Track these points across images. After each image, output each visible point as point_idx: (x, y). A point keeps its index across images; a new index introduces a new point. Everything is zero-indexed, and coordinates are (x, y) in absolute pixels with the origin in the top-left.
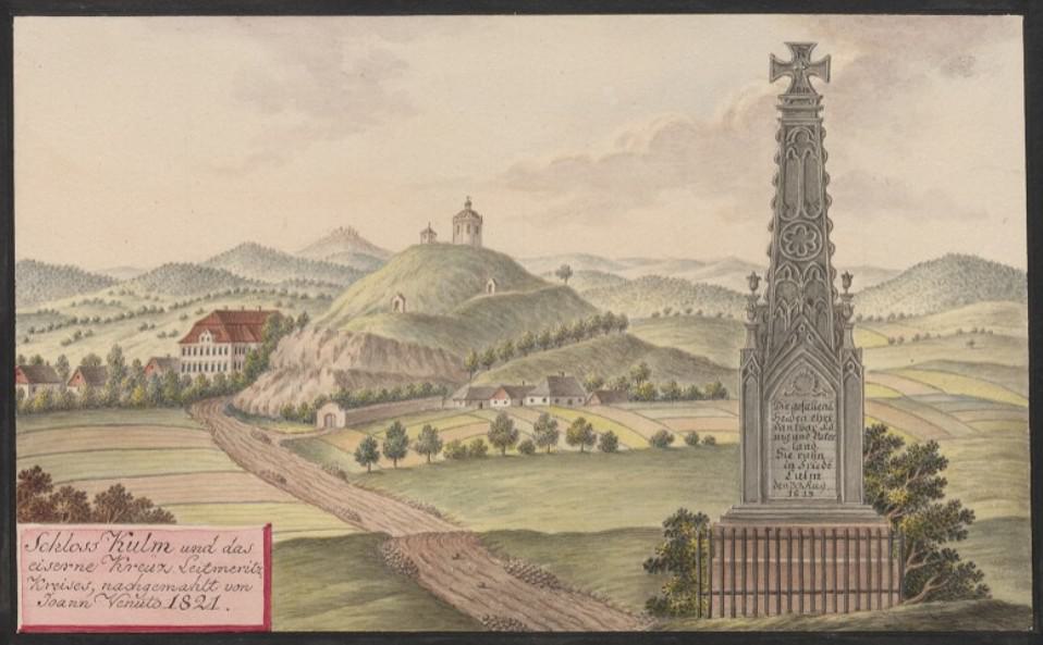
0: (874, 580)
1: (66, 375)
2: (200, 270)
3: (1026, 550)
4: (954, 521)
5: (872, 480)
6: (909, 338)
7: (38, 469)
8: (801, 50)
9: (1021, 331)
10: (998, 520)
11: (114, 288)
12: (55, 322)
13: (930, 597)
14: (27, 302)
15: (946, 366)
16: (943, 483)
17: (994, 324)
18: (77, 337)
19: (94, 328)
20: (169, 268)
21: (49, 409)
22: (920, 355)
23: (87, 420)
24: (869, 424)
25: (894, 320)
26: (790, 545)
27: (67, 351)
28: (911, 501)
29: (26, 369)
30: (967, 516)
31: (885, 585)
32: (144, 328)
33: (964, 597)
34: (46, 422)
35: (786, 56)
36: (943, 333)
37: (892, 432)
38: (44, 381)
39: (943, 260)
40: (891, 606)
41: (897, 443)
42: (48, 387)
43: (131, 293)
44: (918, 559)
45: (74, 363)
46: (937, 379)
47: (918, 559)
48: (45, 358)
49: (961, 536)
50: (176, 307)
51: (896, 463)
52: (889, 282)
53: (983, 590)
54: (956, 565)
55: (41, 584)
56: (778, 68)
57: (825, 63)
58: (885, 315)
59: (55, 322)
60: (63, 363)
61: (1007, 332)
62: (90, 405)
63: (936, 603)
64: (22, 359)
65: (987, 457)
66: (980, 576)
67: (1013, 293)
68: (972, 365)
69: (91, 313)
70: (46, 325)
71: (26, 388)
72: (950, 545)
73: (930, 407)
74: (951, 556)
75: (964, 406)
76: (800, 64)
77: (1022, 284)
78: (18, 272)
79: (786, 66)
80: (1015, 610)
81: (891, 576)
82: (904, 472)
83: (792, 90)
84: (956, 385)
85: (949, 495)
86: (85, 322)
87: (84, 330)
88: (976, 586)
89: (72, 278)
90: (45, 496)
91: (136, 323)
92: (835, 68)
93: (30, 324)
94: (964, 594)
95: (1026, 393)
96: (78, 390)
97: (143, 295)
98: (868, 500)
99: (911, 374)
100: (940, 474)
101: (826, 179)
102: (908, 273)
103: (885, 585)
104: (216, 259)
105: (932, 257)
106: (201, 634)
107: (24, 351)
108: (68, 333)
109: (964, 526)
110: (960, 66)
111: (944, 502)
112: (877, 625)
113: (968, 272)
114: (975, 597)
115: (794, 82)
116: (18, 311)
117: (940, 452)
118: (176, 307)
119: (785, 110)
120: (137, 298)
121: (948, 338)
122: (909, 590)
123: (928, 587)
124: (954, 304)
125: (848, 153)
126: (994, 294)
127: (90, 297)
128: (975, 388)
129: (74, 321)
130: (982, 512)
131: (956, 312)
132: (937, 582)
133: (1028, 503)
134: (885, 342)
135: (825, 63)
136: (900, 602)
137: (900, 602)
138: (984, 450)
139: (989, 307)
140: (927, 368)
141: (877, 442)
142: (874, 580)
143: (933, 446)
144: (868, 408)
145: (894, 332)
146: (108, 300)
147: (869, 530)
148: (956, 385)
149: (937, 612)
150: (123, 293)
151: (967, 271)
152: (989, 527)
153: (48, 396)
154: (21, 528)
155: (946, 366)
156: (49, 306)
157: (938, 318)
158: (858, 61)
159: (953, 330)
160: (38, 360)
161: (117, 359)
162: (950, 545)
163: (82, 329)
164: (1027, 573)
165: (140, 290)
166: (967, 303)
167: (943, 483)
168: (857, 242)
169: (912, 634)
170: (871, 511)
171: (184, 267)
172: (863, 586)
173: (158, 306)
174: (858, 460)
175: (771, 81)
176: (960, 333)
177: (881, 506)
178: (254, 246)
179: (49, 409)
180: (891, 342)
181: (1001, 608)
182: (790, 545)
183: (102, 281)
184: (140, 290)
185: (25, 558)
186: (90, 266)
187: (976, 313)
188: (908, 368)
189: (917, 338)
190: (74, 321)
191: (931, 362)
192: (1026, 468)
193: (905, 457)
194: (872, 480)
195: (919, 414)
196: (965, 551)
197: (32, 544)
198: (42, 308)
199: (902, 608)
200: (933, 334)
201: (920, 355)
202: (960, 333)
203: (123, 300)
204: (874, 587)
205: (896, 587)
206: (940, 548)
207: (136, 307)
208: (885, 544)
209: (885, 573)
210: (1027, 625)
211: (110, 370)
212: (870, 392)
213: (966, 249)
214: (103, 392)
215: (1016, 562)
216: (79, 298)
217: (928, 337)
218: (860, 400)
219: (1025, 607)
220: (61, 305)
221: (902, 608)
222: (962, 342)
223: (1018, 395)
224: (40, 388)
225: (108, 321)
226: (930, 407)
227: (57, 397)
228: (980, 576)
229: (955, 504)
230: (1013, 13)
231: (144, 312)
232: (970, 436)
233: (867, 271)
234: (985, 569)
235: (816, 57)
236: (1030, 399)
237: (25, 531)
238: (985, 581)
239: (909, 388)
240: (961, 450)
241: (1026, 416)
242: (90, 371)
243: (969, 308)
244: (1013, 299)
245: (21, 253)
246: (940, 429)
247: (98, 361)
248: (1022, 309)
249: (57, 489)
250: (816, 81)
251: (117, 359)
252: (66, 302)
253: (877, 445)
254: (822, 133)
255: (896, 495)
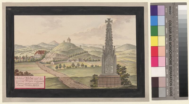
0: (118, 83)
1: (20, 58)
2: (37, 46)
3: (136, 79)
4: (127, 76)
5: (118, 71)
6: (122, 54)
7: (17, 69)
8: (109, 19)
9: (136, 53)
10: (133, 75)
11: (26, 48)
12: (19, 52)
13: (125, 85)
14: (16, 49)
15: (127, 57)
16: (126, 71)
17: (132, 52)
18: (22, 54)
19: (24, 53)
20: (33, 46)
21: (18, 62)
22: (123, 56)
23: (23, 63)
24: (117, 64)
25: (120, 52)
26: (102, 78)
27: (21, 55)
28: (122, 73)
29: (16, 57)
30: (129, 75)
31: (119, 83)
32: (30, 52)
33: (129, 85)
34: (18, 64)
35: (107, 20)
36: (126, 53)
37: (120, 65)
38: (18, 59)
39: (126, 44)
40: (120, 86)
41: (120, 66)
42: (18, 60)
43: (28, 48)
44: (123, 80)
45: (21, 57)
46: (125, 59)
47: (123, 80)
48: (18, 56)
49: (128, 77)
50: (34, 50)
51: (120, 69)
52: (119, 47)
53: (131, 84)
54: (128, 81)
55: (17, 83)
56: (106, 21)
57: (112, 21)
58: (119, 51)
59: (19, 52)
60: (20, 57)
61: (134, 53)
62: (23, 62)
63: (125, 85)
64: (15, 56)
65: (131, 68)
66: (131, 82)
67: (134, 48)
68: (129, 57)
69: (23, 51)
70: (18, 52)
71: (16, 60)
72: (127, 78)
73: (125, 62)
74: (127, 80)
75: (128, 62)
76: (109, 21)
77: (136, 47)
78: (15, 46)
79: (107, 21)
80: (135, 86)
81: (120, 82)
82: (121, 70)
83: (108, 24)
84: (128, 59)
85: (127, 73)
86: (23, 52)
87: (23, 53)
88: (130, 83)
89: (21, 46)
90: (18, 73)
91: (29, 52)
92: (113, 21)
93: (16, 52)
94: (129, 84)
95: (136, 60)
96: (22, 60)
97: (30, 48)
98: (117, 73)
99: (122, 58)
100: (126, 70)
101: (112, 35)
102: (122, 46)
103: (119, 83)
104: (39, 44)
105: (125, 44)
106: (67, 86)
107: (15, 55)
108: (21, 53)
109: (129, 76)
110: (128, 21)
111: (126, 73)
112: (118, 88)
113: (129, 46)
114: (130, 85)
115: (108, 23)
116: (15, 51)
117: (126, 67)
118: (34, 50)
119: (107, 27)
120: (29, 49)
121: (127, 54)
122: (122, 84)
123: (124, 84)
124: (127, 50)
125: (115, 32)
126: (132, 48)
127: (23, 49)
128: (130, 60)
129: (21, 52)
130: (131, 74)
131: (128, 51)
132: (125, 83)
133: (136, 73)
134: (119, 54)
135: (112, 21)
136: (121, 85)
137: (121, 85)
138: (131, 67)
139: (132, 50)
140: (124, 57)
141: (118, 66)
142: (118, 83)
143: (125, 67)
144: (117, 62)
145: (120, 53)
146: (25, 49)
147: (117, 77)
148: (128, 59)
149: (125, 86)
150: (27, 48)
151: (129, 46)
152: (132, 76)
153: (18, 61)
154: (15, 76)
155: (127, 57)
156: (18, 50)
157: (125, 51)
158: (116, 21)
159: (127, 53)
160: (17, 56)
161: (27, 56)
162: (127, 78)
163: (22, 52)
164: (136, 82)
165: (29, 48)
166: (129, 50)
167: (126, 71)
168: (116, 42)
169: (122, 89)
170: (117, 74)
171: (35, 45)
172: (117, 83)
173: (32, 50)
174: (116, 68)
175: (106, 23)
176: (128, 53)
177: (119, 74)
178: (43, 43)
179: (18, 62)
180: (120, 54)
181: (133, 86)
182: (102, 78)
183: (25, 47)
184: (29, 48)
185: (16, 80)
186: (23, 45)
187: (130, 51)
188: (122, 57)
189: (123, 54)
190: (21, 52)
191: (124, 57)
192: (136, 69)
193: (121, 68)
194: (118, 71)
195: (123, 63)
196: (129, 79)
197: (16, 78)
198: (18, 50)
199: (121, 86)
200: (125, 53)
201: (123, 56)
202: (128, 53)
203: (28, 49)
204: (118, 83)
205: (120, 83)
206: (126, 79)
207: (29, 50)
208: (119, 78)
209: (119, 82)
210: (136, 88)
211: (26, 57)
212: (117, 60)
213: (129, 43)
214: (25, 60)
215: (135, 80)
216: (22, 49)
217: (124, 54)
218: (116, 61)
219: (136, 86)
220: (20, 50)
221: (121, 86)
222: (128, 54)
223: (135, 61)
224: (17, 60)
225: (26, 52)
226: (125, 62)
227: (19, 61)
228: (131, 82)
229: (128, 74)
230: (134, 15)
231: (30, 51)
232: (129, 65)
233: (117, 46)
234: (131, 81)
235: (111, 20)
236: (137, 61)
237: (16, 77)
238: (131, 83)
239: (122, 60)
240: (128, 67)
241: (136, 63)
242: (23, 58)
243: (129, 50)
244: (134, 49)
245: (15, 44)
246: (126, 65)
247: (24, 56)
248: (135, 50)
249: (19, 72)
250: (111, 23)
251: (27, 56)
252: (21, 49)
253: (118, 67)
254: (112, 29)
255: (120, 73)
